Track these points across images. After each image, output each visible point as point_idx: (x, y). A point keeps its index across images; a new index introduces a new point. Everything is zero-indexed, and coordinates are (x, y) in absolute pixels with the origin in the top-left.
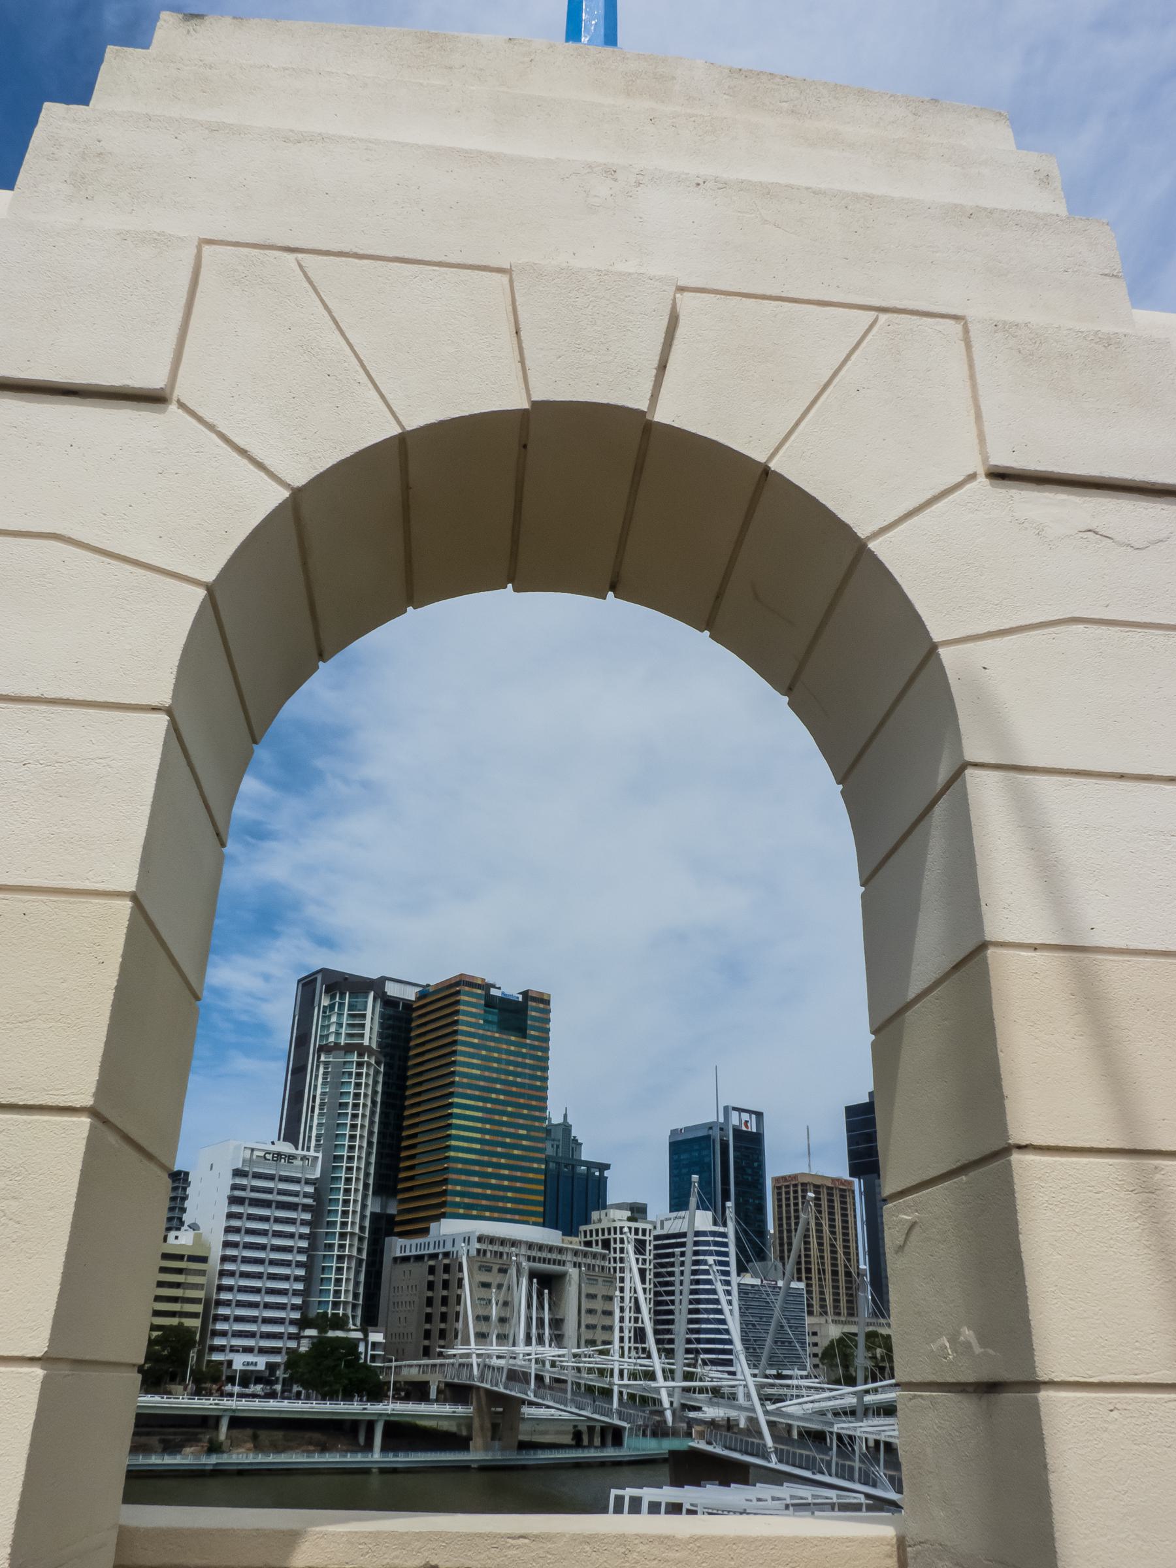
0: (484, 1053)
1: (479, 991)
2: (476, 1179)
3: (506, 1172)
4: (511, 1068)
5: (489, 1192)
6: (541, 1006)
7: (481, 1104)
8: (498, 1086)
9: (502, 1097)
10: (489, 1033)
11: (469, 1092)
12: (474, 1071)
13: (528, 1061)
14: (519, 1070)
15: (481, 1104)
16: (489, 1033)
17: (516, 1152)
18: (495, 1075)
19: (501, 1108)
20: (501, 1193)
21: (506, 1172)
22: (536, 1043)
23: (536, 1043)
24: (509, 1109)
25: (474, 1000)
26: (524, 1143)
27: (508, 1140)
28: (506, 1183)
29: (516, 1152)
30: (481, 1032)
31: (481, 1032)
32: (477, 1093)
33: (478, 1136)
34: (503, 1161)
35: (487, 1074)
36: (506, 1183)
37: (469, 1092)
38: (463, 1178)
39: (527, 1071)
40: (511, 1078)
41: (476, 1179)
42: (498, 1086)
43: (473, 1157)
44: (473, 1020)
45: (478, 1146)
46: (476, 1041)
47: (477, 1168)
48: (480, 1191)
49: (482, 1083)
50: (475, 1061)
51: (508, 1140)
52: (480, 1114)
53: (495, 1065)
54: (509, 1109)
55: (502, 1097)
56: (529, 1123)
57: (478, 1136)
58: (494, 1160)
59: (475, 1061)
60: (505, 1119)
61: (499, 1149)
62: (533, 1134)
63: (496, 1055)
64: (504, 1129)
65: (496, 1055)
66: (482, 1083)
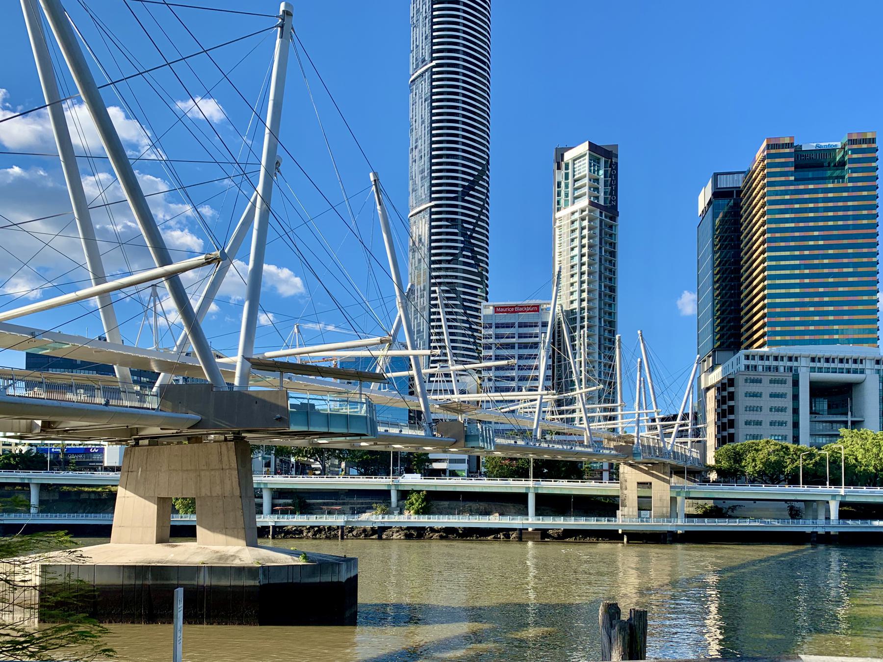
0: (797, 206)
1: (787, 150)
2: (797, 319)
3: (831, 308)
4: (831, 214)
5: (812, 328)
6: (864, 146)
7: (797, 253)
8: (816, 233)
9: (821, 243)
10: (802, 187)
11: (783, 244)
12: (787, 225)
13: (850, 203)
14: (840, 213)
15: (797, 253)
16: (802, 187)
17: (841, 289)
18: (811, 224)
19: (821, 252)
20: (827, 327)
21: (831, 308)
22: (860, 184)
23: (860, 184)
24: (831, 252)
25: (783, 160)
26: (850, 279)
27: (831, 280)
28: (831, 318)
29: (841, 289)
30: (792, 188)
31: (792, 188)
32: (792, 244)
33: (797, 281)
34: (826, 299)
35: (801, 225)
36: (831, 318)
37: (783, 244)
38: (783, 319)
39: (850, 213)
40: (831, 223)
41: (797, 319)
42: (816, 233)
43: (793, 300)
44: (783, 179)
45: (797, 290)
46: (787, 197)
47: (797, 309)
48: (802, 328)
49: (797, 234)
50: (787, 216)
51: (831, 280)
52: (797, 262)
53: (811, 215)
54: (831, 252)
55: (821, 243)
56: (856, 260)
57: (797, 281)
58: (816, 299)
59: (787, 216)
60: (826, 261)
61: (821, 290)
62: (860, 270)
63: (811, 205)
64: (826, 271)
65: (811, 205)
66: (797, 234)
